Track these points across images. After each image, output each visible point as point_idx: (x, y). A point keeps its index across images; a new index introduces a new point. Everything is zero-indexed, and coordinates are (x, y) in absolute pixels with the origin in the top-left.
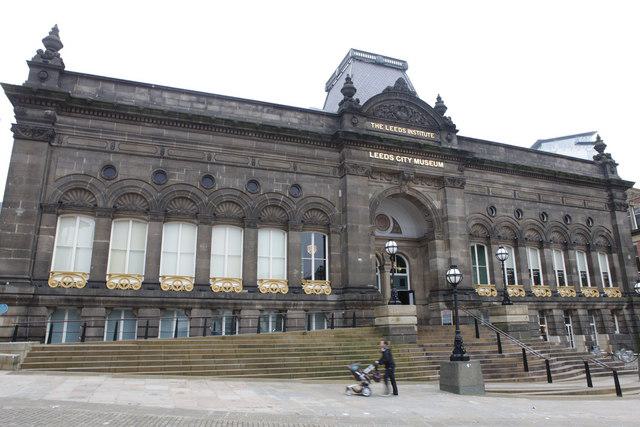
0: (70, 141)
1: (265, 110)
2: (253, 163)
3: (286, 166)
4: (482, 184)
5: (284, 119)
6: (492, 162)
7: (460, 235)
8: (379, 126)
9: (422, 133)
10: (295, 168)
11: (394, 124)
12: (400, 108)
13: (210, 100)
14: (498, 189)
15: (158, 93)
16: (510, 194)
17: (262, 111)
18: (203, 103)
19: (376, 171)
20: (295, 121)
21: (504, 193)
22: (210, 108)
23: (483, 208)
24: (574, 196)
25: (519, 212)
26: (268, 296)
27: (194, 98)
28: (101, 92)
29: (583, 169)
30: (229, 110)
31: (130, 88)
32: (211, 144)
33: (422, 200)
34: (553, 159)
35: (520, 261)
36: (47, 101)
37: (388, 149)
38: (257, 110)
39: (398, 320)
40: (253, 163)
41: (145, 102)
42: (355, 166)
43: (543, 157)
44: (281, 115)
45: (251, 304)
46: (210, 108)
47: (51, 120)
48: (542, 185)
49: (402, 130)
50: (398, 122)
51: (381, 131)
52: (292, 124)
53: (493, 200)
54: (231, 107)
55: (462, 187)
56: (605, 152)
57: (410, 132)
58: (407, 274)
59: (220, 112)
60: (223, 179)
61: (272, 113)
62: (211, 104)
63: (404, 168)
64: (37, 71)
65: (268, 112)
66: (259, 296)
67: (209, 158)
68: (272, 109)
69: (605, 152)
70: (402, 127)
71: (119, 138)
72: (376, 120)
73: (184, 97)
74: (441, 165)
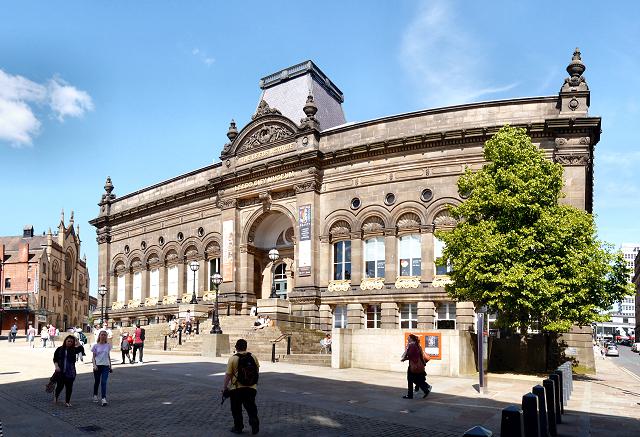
12: (265, 132)
22: (162, 192)
23: (345, 202)
25: (390, 197)
35: (391, 252)
37: (247, 179)
46: (162, 192)
60: (167, 238)
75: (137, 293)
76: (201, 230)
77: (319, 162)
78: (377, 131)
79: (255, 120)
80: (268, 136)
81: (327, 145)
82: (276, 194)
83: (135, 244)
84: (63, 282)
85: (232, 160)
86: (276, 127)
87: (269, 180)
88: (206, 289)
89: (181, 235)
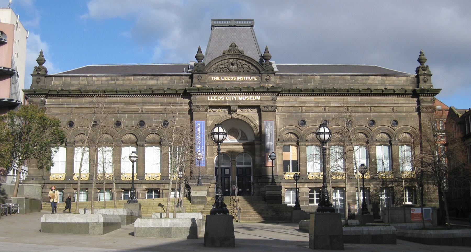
0: (53, 111)
1: (149, 77)
2: (142, 111)
3: (161, 110)
4: (296, 105)
5: (159, 82)
9: (248, 78)
10: (165, 111)
11: (227, 74)
13: (118, 78)
15: (90, 78)
16: (321, 109)
17: (146, 79)
18: (114, 80)
20: (166, 82)
21: (315, 110)
22: (118, 82)
24: (382, 105)
26: (150, 182)
27: (109, 78)
28: (64, 83)
29: (396, 82)
30: (128, 82)
31: (78, 78)
32: (118, 103)
33: (248, 121)
34: (367, 77)
36: (41, 94)
37: (220, 93)
38: (143, 79)
39: (196, 193)
40: (142, 111)
41: (85, 86)
42: (199, 107)
43: (356, 77)
44: (157, 80)
45: (140, 186)
46: (118, 82)
47: (44, 102)
48: (351, 99)
50: (230, 72)
51: (218, 81)
52: (163, 84)
53: (304, 116)
54: (129, 80)
55: (275, 110)
56: (425, 65)
57: (239, 78)
58: (252, 166)
59: (122, 85)
60: (124, 122)
61: (152, 79)
62: (117, 80)
63: (231, 104)
64: (36, 78)
65: (150, 80)
66: (144, 182)
67: (118, 111)
68: (152, 77)
69: (425, 65)
70: (233, 76)
71: (74, 106)
72: (214, 73)
73: (104, 78)
74: (258, 98)
78: (314, 80)
85: (204, 76)
86: (244, 62)
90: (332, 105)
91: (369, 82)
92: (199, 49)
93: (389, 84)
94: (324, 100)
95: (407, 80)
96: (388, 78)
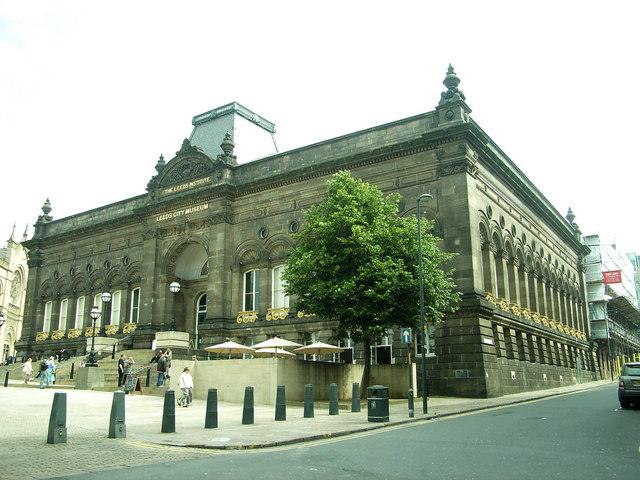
6: (274, 178)
7: (218, 268)
8: (170, 191)
9: (201, 181)
14: (275, 205)
19: (162, 232)
43: (340, 143)
49: (185, 186)
54: (104, 213)
57: (191, 184)
73: (85, 217)
74: (206, 207)
75: (62, 324)
76: (126, 259)
77: (231, 193)
79: (178, 154)
80: (188, 171)
81: (242, 179)
82: (192, 225)
83: (64, 270)
84: (6, 305)
87: (187, 212)
88: (127, 321)
89: (107, 263)
90: (303, 196)
91: (359, 145)
92: (162, 158)
93: (390, 141)
94: (291, 192)
95: (421, 125)
96: (389, 130)
